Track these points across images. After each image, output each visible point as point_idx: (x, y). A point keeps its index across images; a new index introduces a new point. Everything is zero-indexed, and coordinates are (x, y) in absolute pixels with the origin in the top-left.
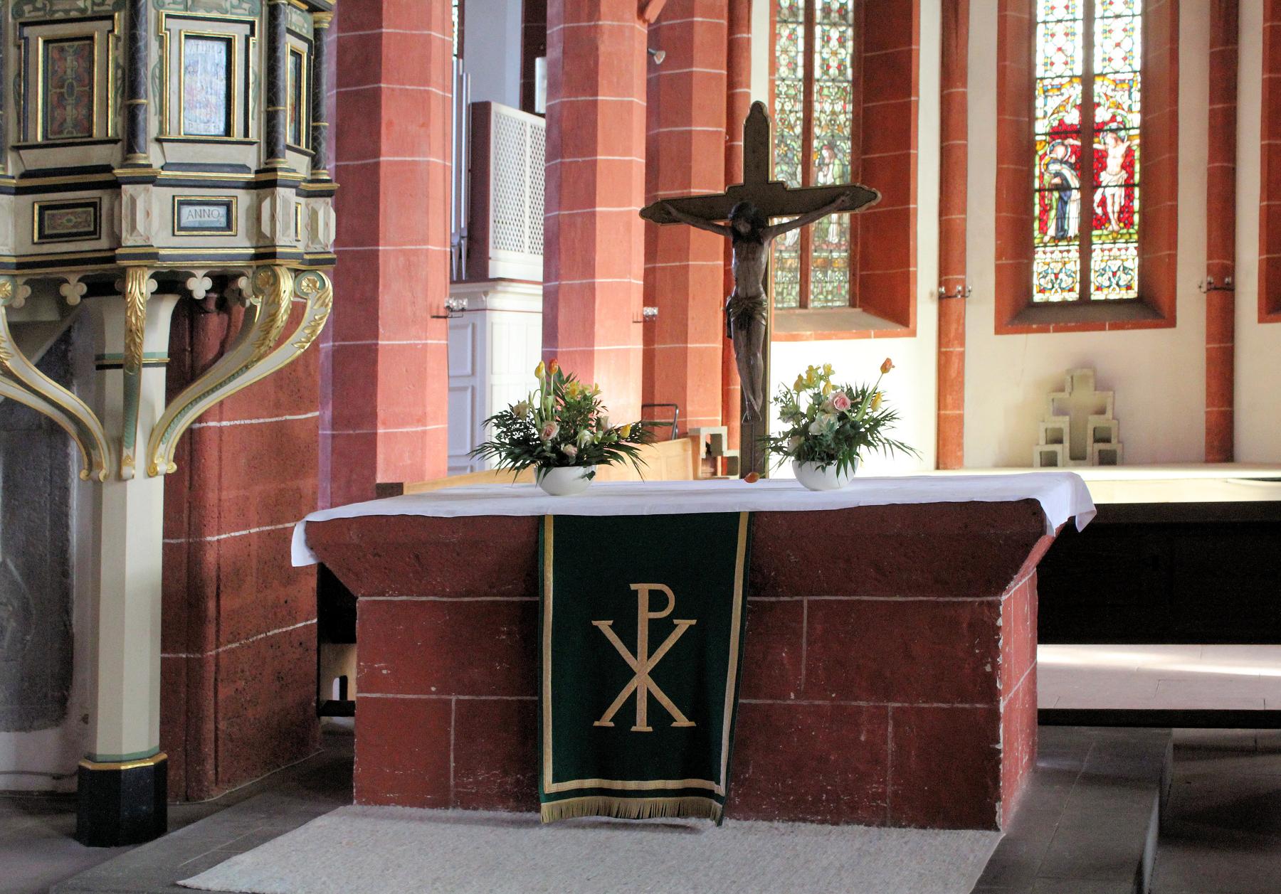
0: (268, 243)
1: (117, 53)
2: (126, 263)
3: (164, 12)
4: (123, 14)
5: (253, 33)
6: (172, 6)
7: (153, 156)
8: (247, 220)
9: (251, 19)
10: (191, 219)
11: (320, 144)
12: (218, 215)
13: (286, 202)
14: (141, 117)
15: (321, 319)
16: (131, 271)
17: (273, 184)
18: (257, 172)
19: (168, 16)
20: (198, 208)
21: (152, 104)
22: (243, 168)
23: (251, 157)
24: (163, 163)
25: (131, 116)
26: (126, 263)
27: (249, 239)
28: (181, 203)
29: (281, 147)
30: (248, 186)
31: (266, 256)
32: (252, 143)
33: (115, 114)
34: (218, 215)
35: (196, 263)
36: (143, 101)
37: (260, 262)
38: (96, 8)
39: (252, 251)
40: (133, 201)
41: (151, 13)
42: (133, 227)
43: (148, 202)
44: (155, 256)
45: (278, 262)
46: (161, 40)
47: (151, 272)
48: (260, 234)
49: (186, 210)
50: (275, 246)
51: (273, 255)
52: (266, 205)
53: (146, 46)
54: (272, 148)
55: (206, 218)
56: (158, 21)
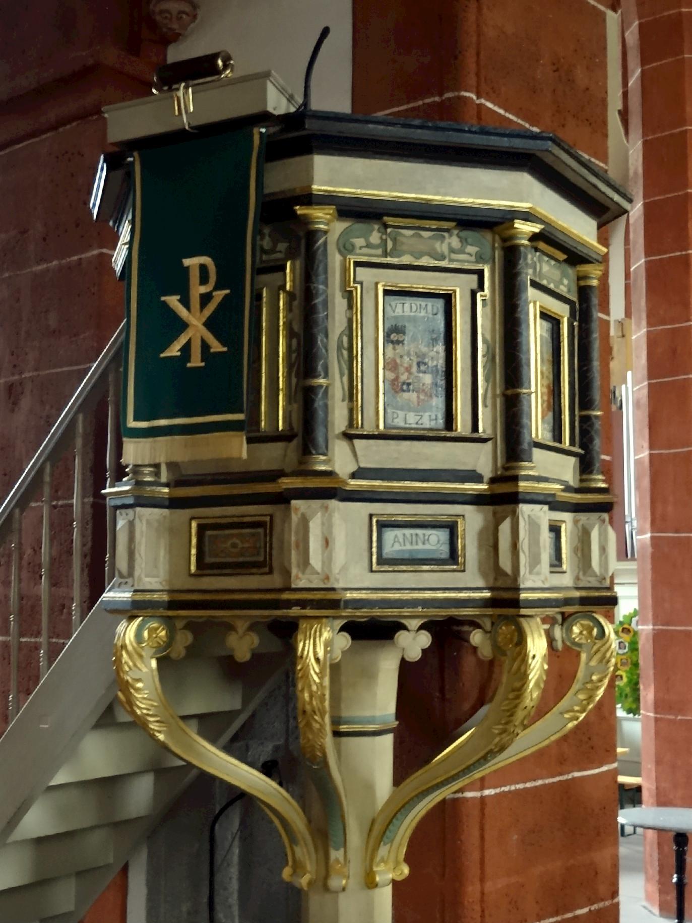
0: (509, 583)
1: (290, 316)
2: (295, 611)
3: (353, 259)
4: (298, 263)
5: (481, 287)
6: (365, 251)
7: (340, 460)
8: (480, 547)
9: (479, 267)
10: (397, 547)
11: (591, 440)
12: (436, 541)
13: (534, 526)
14: (319, 403)
15: (600, 680)
16: (303, 625)
17: (514, 499)
18: (493, 481)
19: (357, 264)
20: (408, 532)
21: (338, 384)
22: (475, 477)
23: (482, 459)
24: (353, 468)
25: (307, 400)
26: (295, 611)
27: (483, 573)
28: (382, 526)
29: (525, 446)
30: (477, 500)
31: (506, 601)
32: (484, 440)
33: (289, 399)
34: (436, 541)
35: (406, 611)
36: (321, 381)
37: (498, 611)
38: (264, 257)
39: (487, 594)
40: (305, 522)
41: (335, 260)
42: (305, 562)
43: (328, 527)
44: (334, 604)
45: (524, 611)
46: (349, 296)
47: (339, 623)
48: (498, 571)
49: (390, 535)
50: (517, 589)
51: (516, 603)
52: (505, 528)
53: (325, 303)
54: (513, 443)
55: (420, 546)
56: (345, 270)
